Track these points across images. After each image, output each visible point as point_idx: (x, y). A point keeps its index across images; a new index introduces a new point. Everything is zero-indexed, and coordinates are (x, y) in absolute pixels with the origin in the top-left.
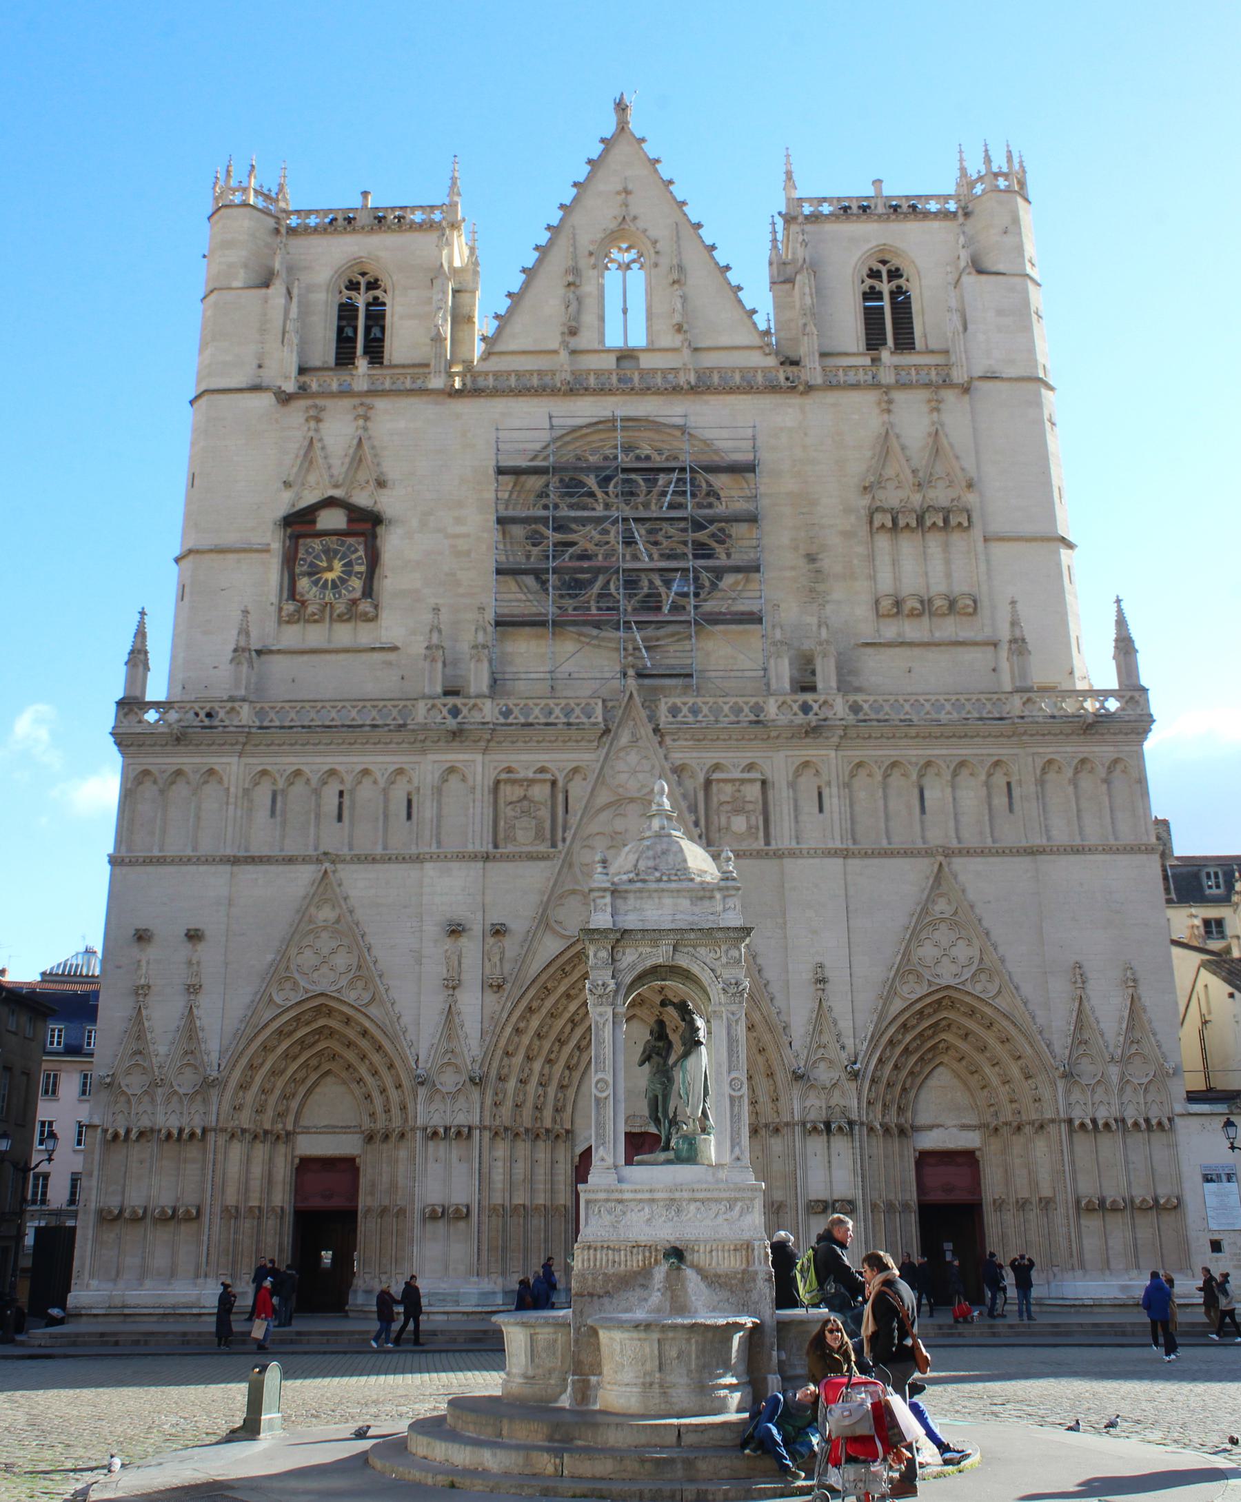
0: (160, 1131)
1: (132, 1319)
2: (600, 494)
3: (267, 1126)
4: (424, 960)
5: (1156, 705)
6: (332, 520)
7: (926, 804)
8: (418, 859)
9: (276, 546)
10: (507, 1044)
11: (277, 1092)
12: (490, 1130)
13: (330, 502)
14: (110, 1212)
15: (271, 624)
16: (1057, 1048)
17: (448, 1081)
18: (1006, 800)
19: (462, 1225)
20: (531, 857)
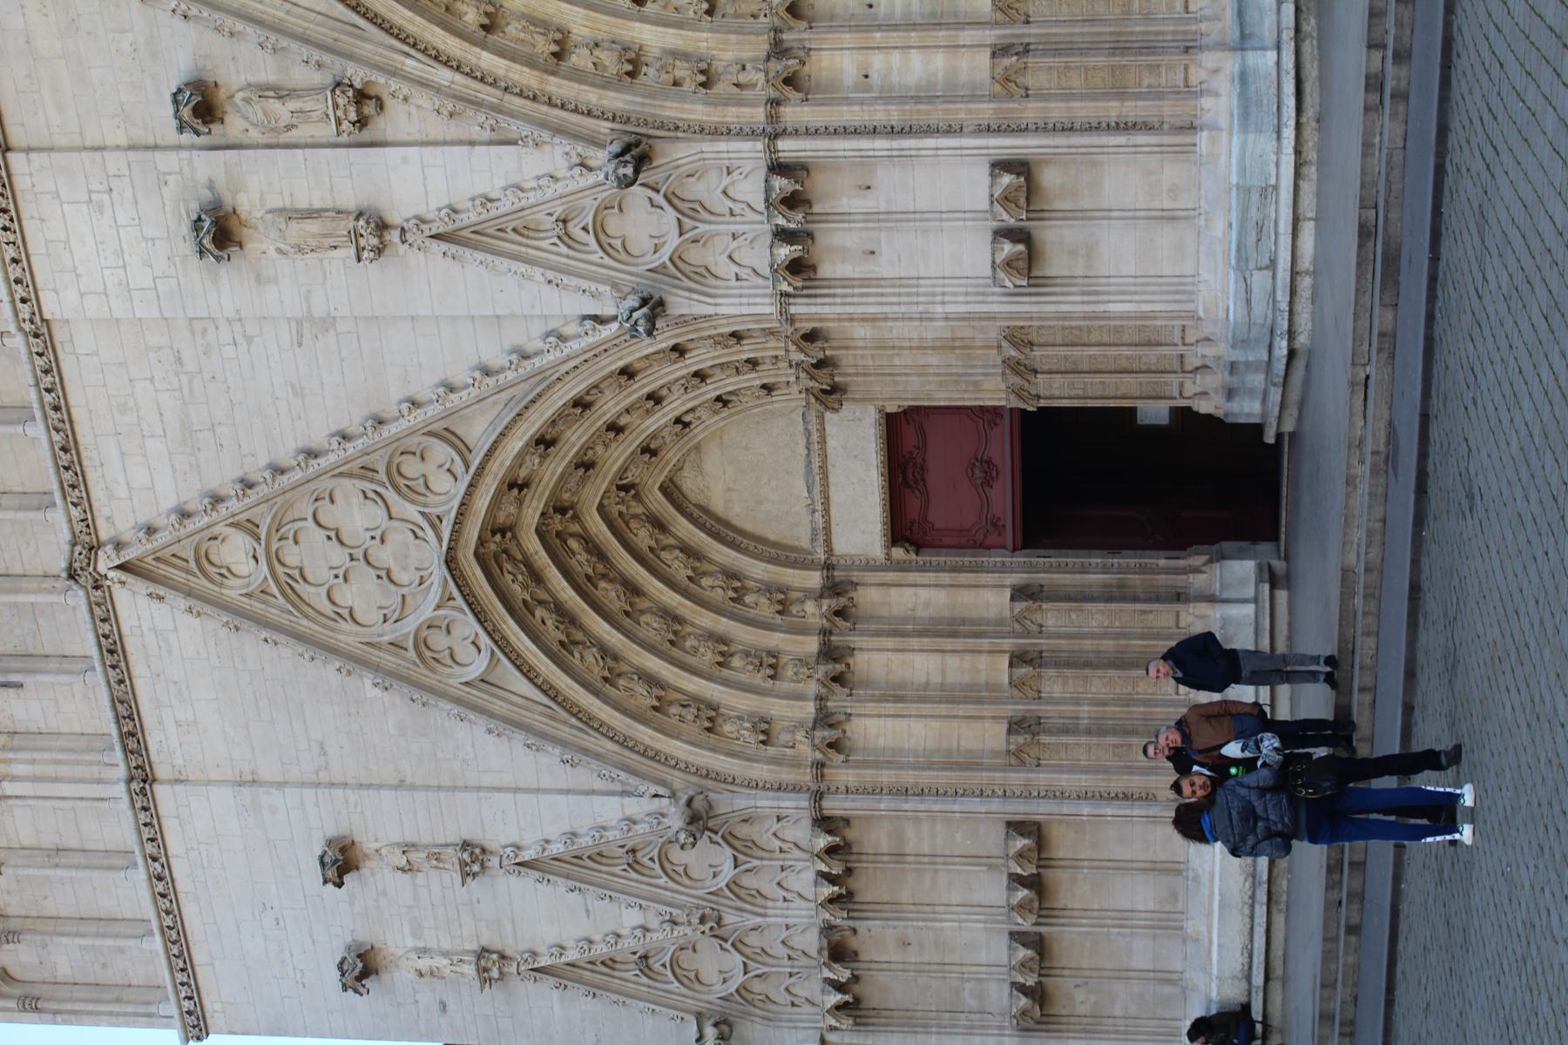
1: (1278, 970)
3: (812, 645)
4: (319, 311)
10: (531, 63)
11: (724, 625)
12: (775, 103)
19: (1050, 178)
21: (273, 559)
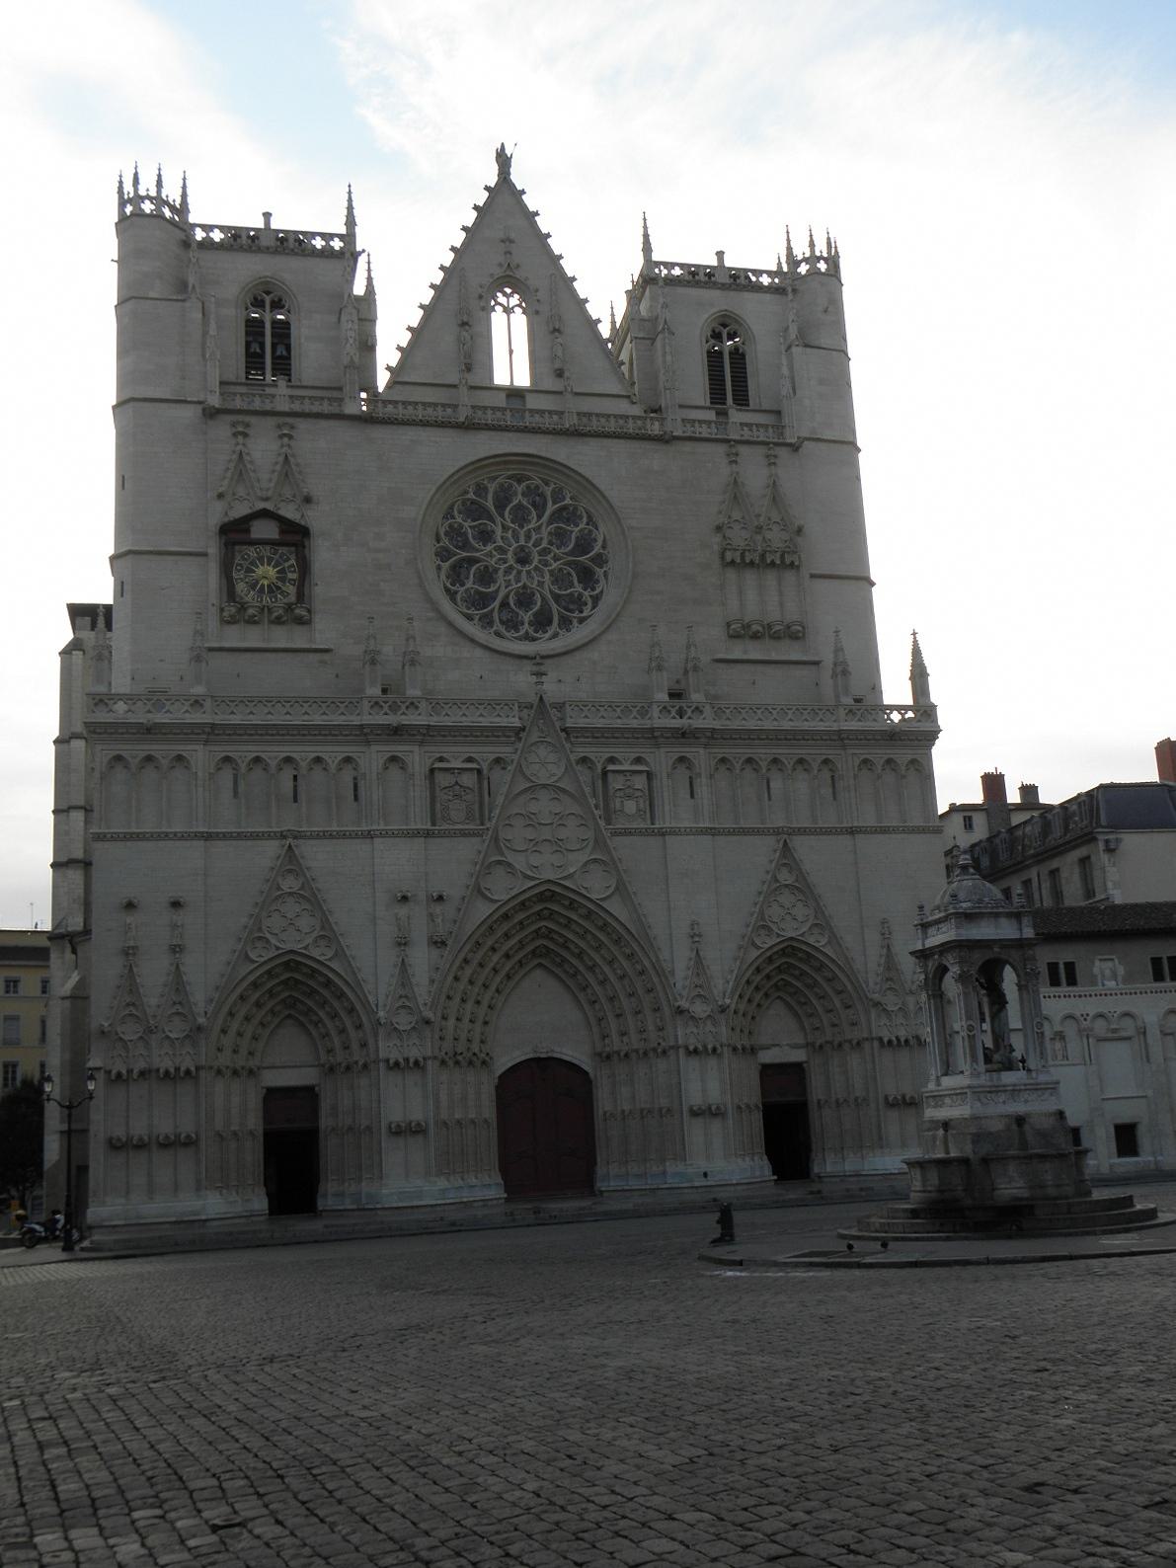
0: (158, 1070)
2: (499, 519)
5: (942, 721)
6: (264, 530)
7: (772, 791)
8: (369, 836)
9: (213, 549)
13: (264, 514)
14: (119, 1140)
15: (213, 623)
16: (871, 984)
17: (404, 1021)
18: (831, 790)
19: (420, 1138)
20: (464, 834)
21: (291, 894)
